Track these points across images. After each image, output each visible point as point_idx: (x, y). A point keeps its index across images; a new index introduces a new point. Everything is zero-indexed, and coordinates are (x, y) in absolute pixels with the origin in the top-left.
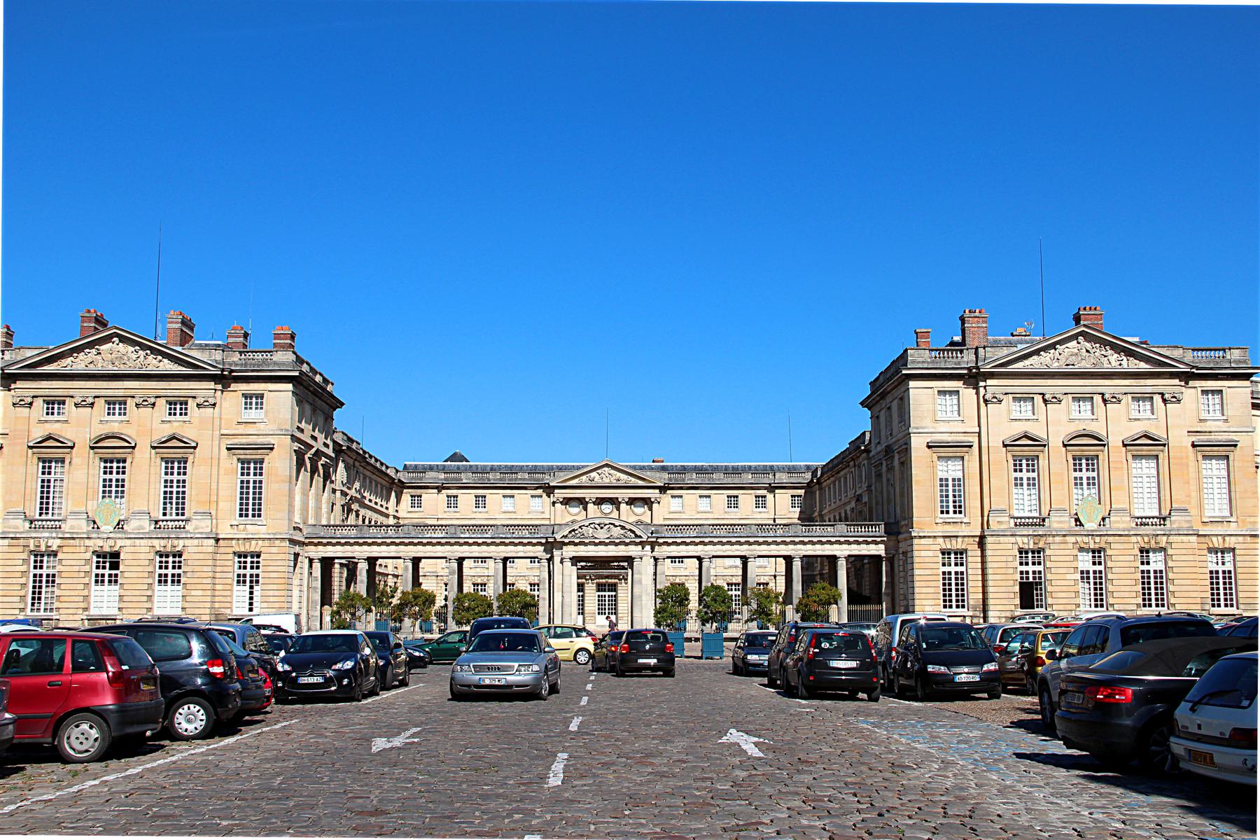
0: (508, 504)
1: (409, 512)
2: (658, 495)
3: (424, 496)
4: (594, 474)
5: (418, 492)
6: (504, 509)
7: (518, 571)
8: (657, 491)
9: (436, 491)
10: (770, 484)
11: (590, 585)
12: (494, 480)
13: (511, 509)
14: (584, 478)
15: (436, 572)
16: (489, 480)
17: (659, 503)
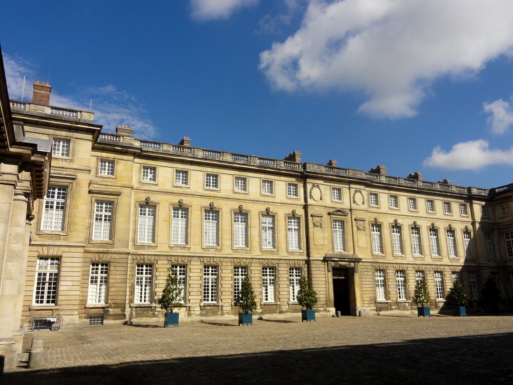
1: (501, 218)
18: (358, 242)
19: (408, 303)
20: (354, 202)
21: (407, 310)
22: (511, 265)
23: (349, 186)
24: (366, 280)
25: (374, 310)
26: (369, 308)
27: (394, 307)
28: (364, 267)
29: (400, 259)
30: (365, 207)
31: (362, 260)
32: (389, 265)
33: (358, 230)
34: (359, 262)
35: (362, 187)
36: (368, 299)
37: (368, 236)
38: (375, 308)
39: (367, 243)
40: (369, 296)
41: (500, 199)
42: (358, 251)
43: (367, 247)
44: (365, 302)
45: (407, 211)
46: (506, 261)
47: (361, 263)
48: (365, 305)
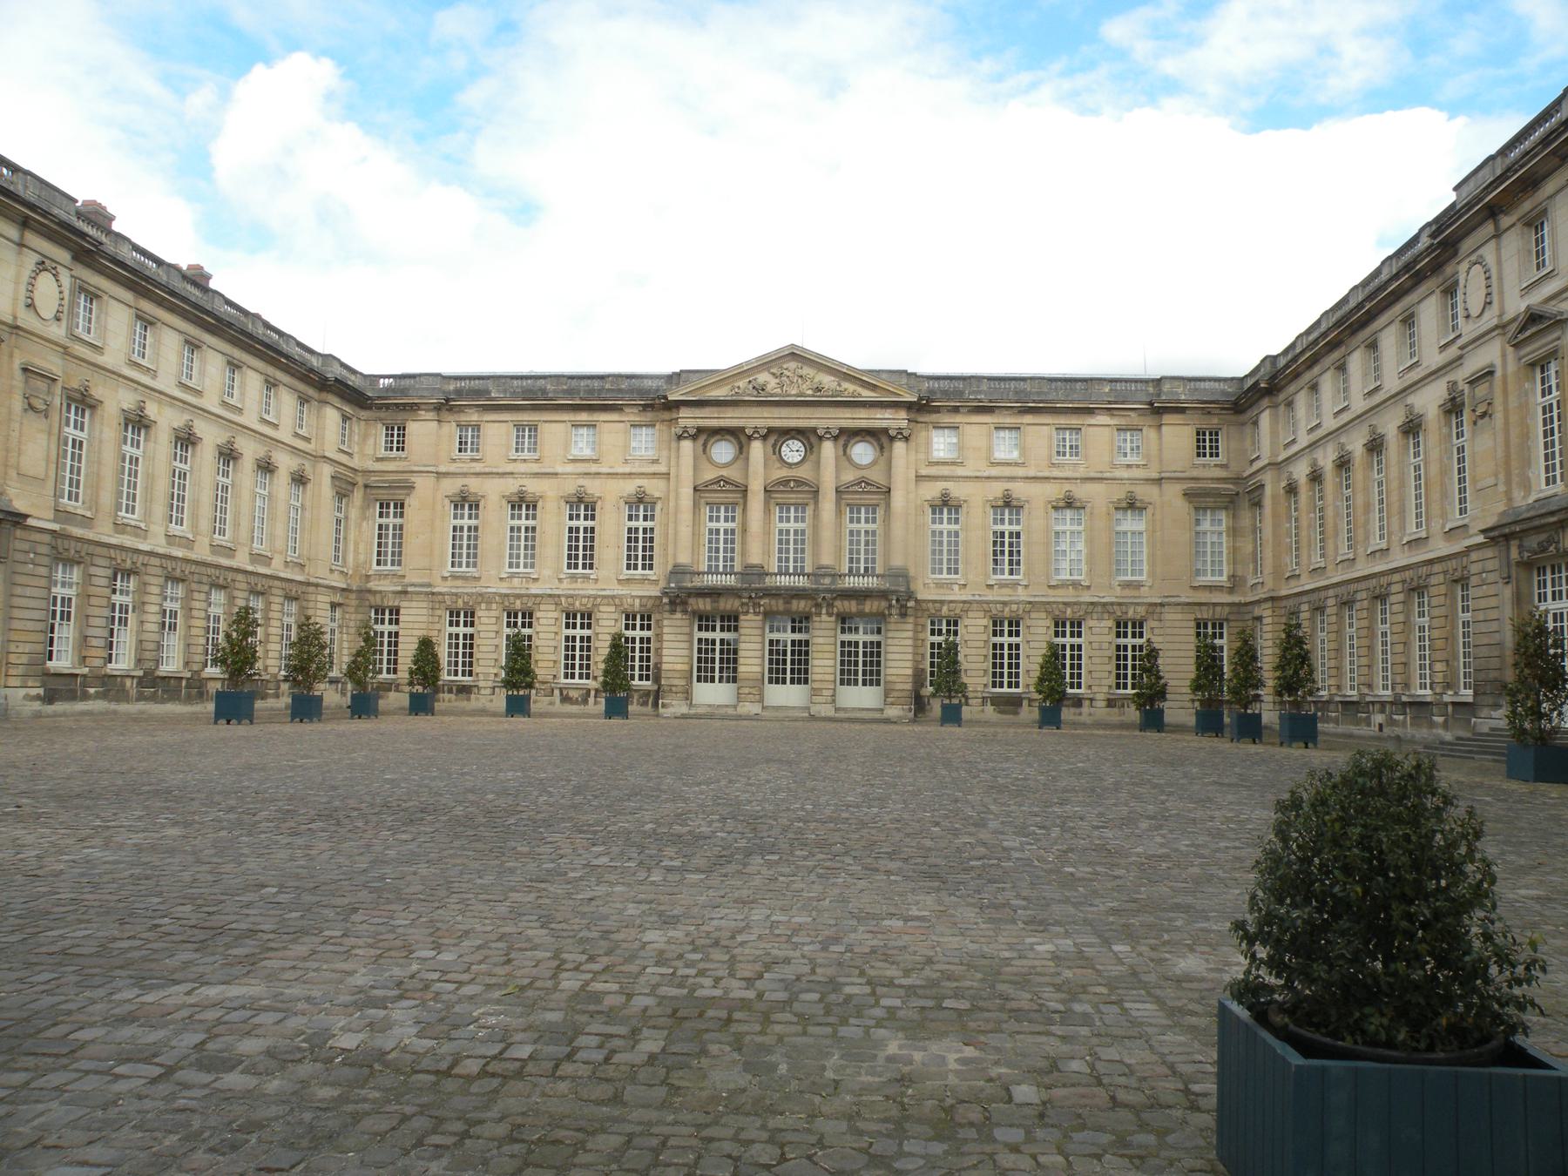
0: (582, 445)
1: (379, 460)
2: (904, 424)
3: (413, 428)
4: (763, 377)
5: (401, 416)
6: (575, 452)
7: (600, 586)
8: (903, 414)
9: (431, 415)
10: (1151, 404)
11: (750, 617)
12: (555, 391)
13: (587, 453)
14: (742, 384)
15: (430, 585)
16: (544, 391)
17: (907, 439)
18: (19, 455)
19: (133, 677)
20: (31, 306)
21: (127, 699)
22: (379, 588)
23: (22, 236)
24: (28, 591)
25: (38, 697)
26: (22, 692)
27: (92, 691)
28: (26, 546)
29: (129, 534)
30: (58, 332)
31: (30, 522)
32: (99, 550)
33: (25, 410)
34: (16, 524)
35: (63, 256)
36: (24, 659)
37: (54, 439)
38: (41, 691)
39: (48, 461)
40: (27, 648)
41: (388, 407)
42: (18, 485)
43: (47, 475)
44: (11, 672)
45: (173, 381)
46: (368, 577)
47: (19, 533)
48: (13, 682)
